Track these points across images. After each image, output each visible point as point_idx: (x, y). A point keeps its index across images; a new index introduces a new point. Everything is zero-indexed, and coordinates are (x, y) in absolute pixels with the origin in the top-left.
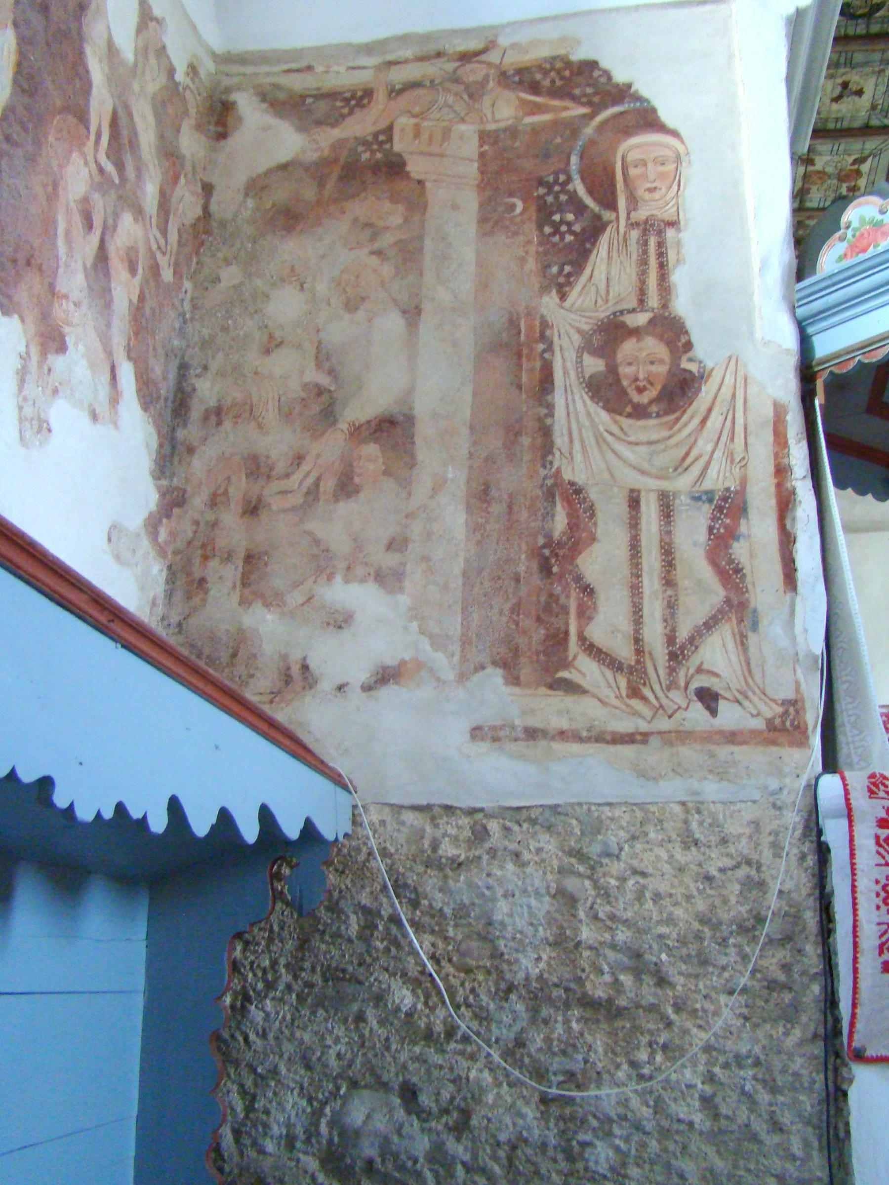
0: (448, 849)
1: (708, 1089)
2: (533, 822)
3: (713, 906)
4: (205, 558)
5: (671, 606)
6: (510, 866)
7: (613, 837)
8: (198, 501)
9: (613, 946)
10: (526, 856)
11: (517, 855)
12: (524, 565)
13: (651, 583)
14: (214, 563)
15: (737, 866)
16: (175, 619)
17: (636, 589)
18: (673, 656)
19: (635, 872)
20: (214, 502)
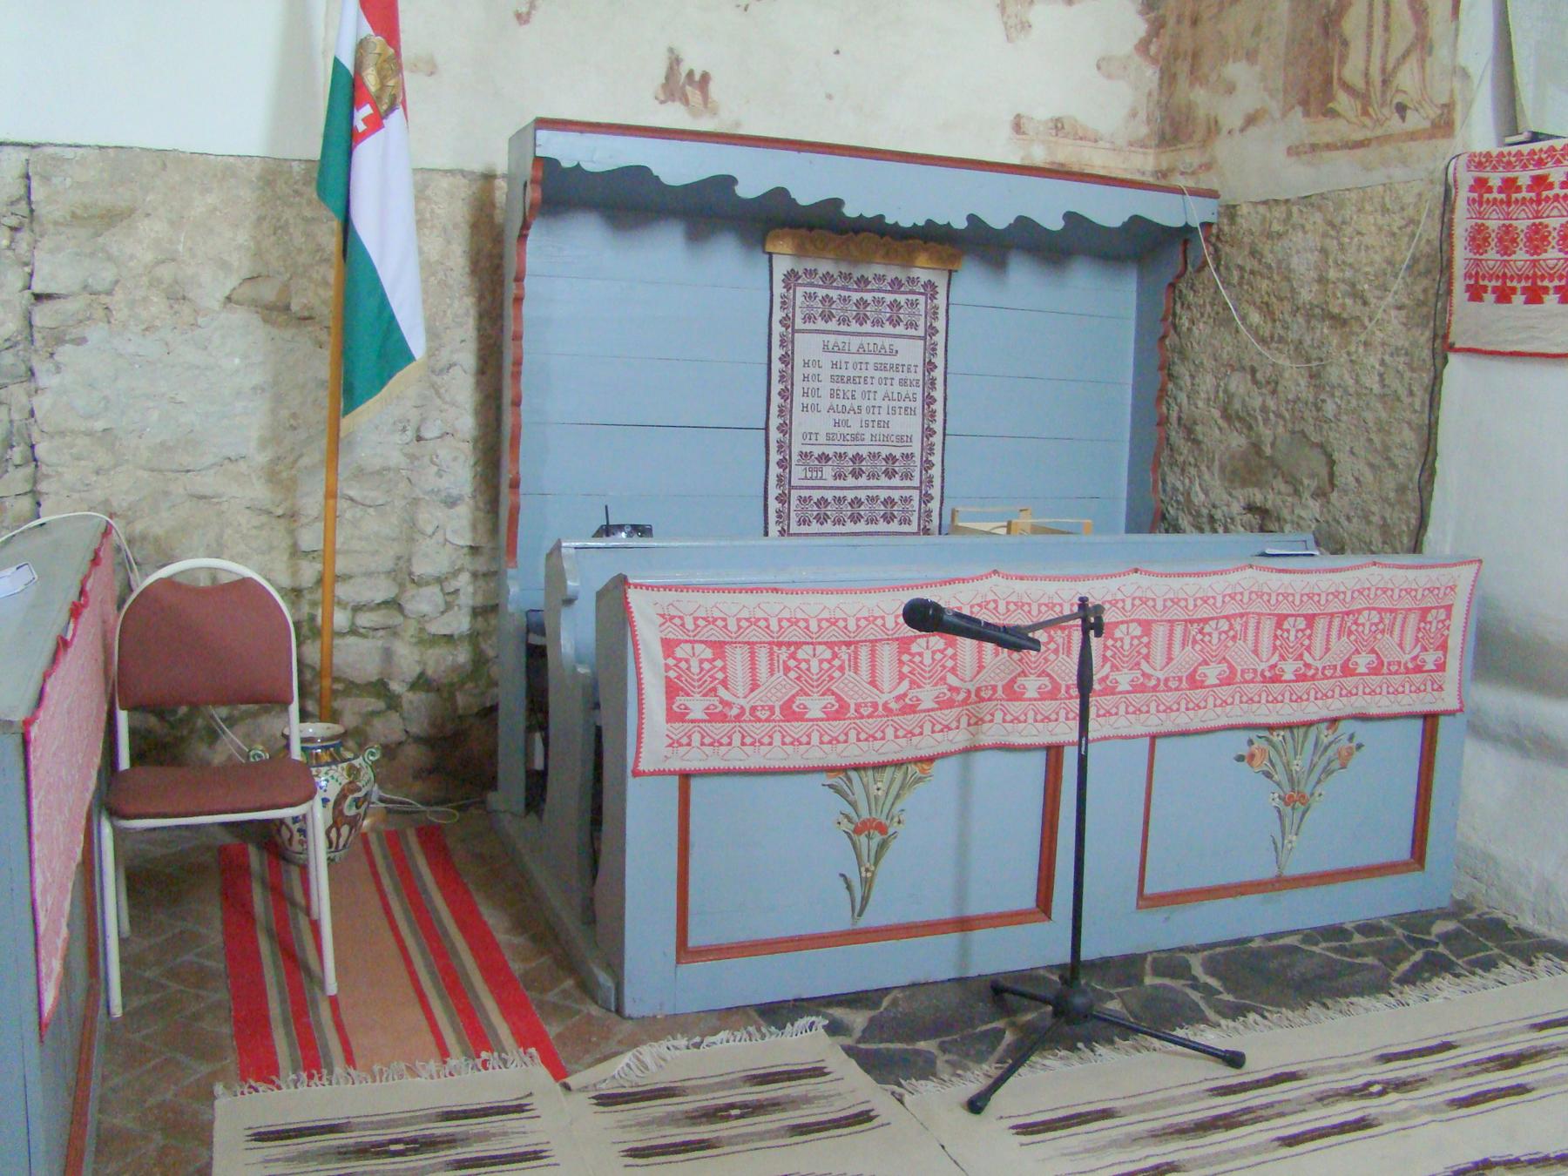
0: (1276, 227)
1: (1382, 369)
2: (1312, 205)
3: (1393, 253)
4: (1176, 59)
5: (1387, 46)
6: (1300, 234)
7: (1348, 212)
8: (1171, 21)
9: (1344, 281)
10: (1308, 227)
11: (1303, 227)
12: (1315, 32)
13: (1378, 30)
14: (1179, 62)
15: (1407, 225)
16: (1164, 100)
17: (1369, 36)
18: (1385, 82)
19: (1359, 233)
20: (1179, 22)
